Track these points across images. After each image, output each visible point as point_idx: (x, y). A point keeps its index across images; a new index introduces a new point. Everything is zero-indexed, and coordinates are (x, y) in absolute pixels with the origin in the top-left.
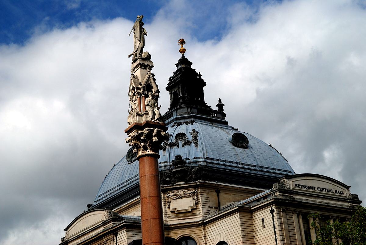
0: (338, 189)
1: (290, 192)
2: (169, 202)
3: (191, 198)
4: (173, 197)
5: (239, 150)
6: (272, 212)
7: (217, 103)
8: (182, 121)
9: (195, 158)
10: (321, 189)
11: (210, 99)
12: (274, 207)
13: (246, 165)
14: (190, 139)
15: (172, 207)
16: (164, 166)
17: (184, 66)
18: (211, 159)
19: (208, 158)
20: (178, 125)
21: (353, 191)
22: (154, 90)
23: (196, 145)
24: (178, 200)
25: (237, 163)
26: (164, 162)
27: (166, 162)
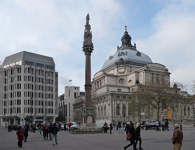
0: (162, 67)
1: (149, 68)
6: (144, 73)
10: (158, 67)
11: (133, 44)
21: (166, 68)
22: (90, 36)
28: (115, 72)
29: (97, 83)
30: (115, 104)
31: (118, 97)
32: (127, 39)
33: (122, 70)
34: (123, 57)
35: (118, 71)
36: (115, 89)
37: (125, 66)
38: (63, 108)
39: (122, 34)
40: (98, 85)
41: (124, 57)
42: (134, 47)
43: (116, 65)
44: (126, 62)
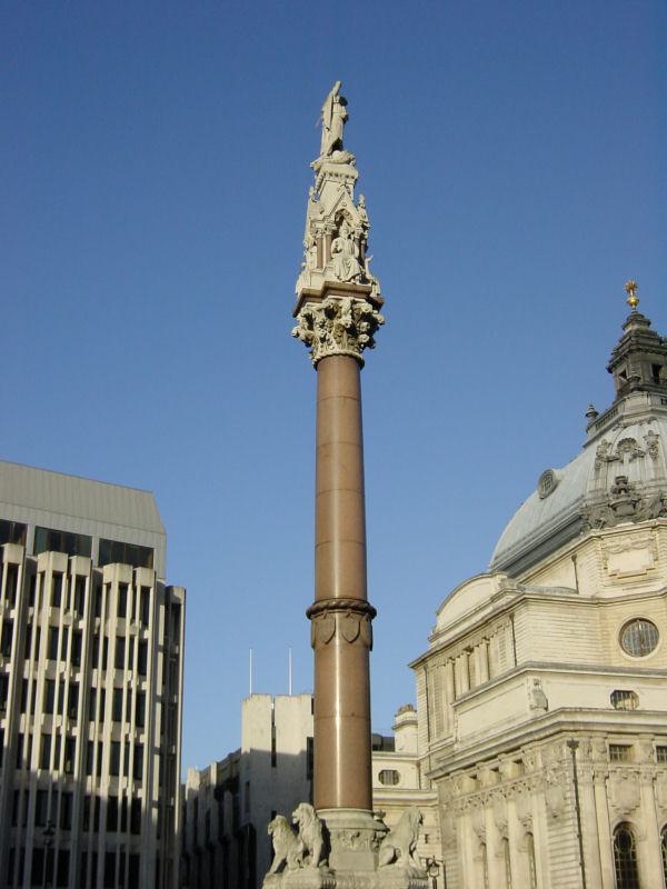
3: (646, 551)
14: (644, 447)
15: (610, 571)
17: (636, 327)
23: (655, 457)
24: (622, 555)
34: (634, 471)
36: (596, 695)
38: (234, 846)
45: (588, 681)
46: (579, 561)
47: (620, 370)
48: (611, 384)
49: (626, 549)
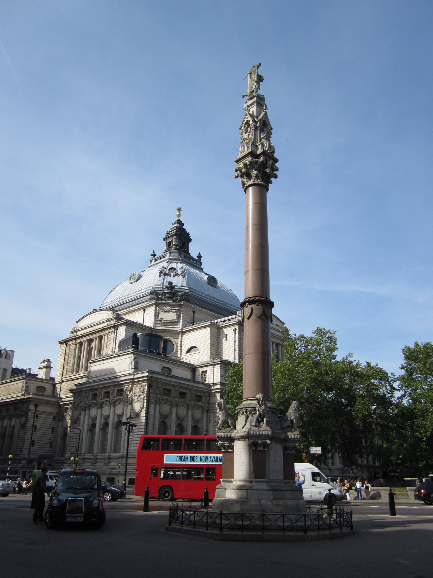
2: (159, 313)
3: (175, 313)
4: (162, 310)
5: (211, 287)
6: (235, 330)
7: (198, 255)
8: (173, 261)
9: (181, 286)
12: (237, 327)
13: (215, 298)
15: (160, 317)
16: (158, 288)
18: (192, 289)
19: (190, 288)
20: (170, 263)
25: (209, 296)
26: (159, 285)
27: (160, 285)
28: (147, 318)
29: (85, 346)
30: (157, 415)
31: (183, 395)
32: (180, 240)
33: (171, 316)
35: (156, 317)
37: (180, 306)
39: (169, 226)
40: (90, 351)
41: (180, 282)
42: (198, 263)
43: (151, 299)
44: (183, 295)
45: (154, 361)
46: (146, 312)
47: (169, 240)
48: (164, 246)
49: (168, 311)
